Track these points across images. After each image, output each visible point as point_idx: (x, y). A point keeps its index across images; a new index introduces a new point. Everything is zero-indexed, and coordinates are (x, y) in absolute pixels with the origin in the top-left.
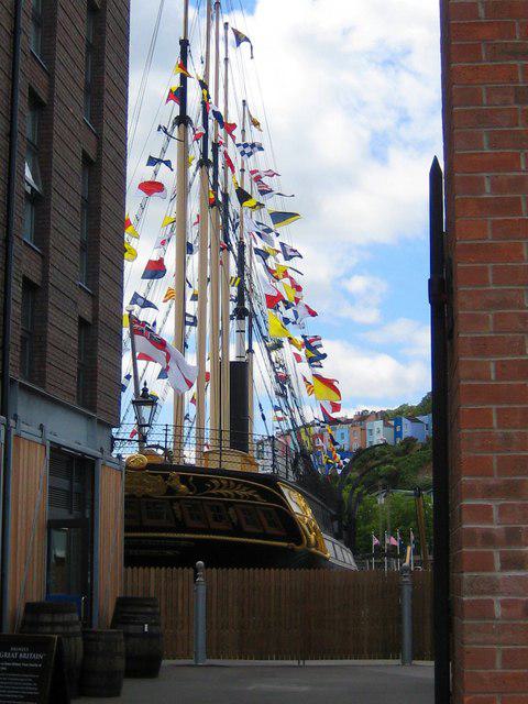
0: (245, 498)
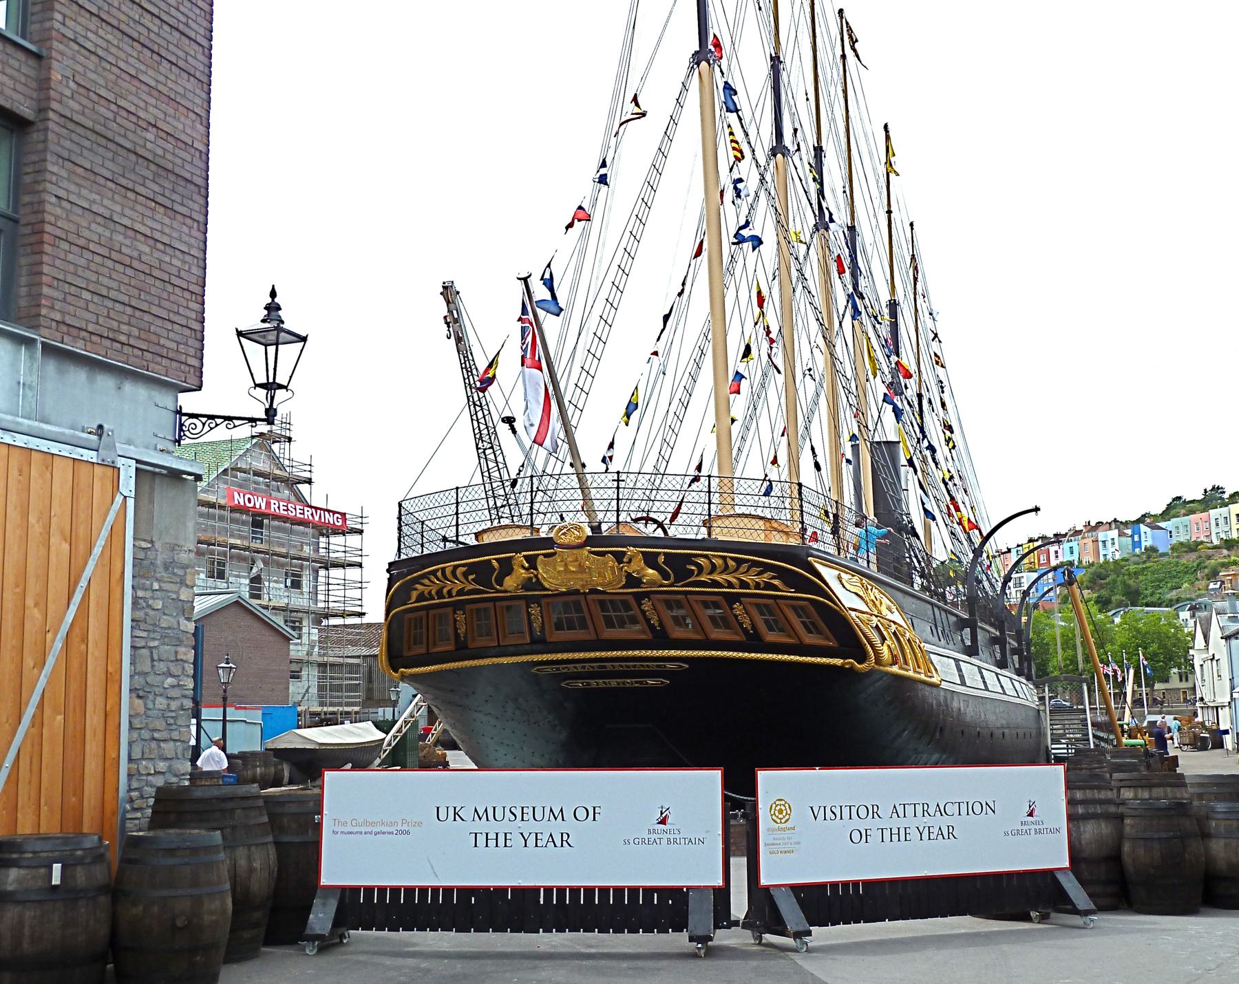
0: (757, 586)
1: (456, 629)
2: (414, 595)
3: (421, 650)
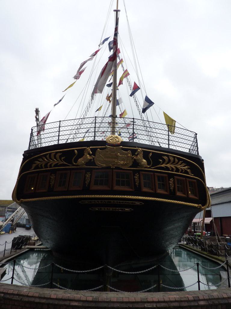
1: (50, 182)
2: (34, 166)
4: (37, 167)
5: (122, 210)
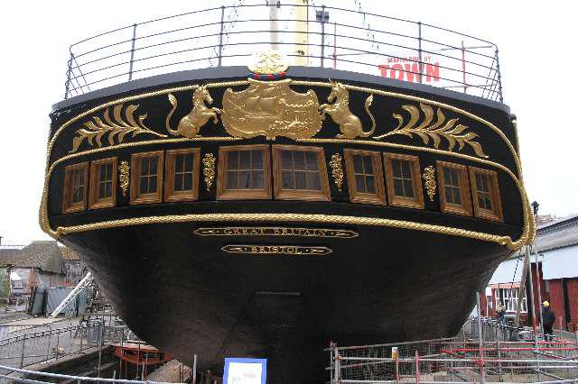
2: (77, 142)
3: (79, 207)
4: (84, 145)
5: (304, 251)
